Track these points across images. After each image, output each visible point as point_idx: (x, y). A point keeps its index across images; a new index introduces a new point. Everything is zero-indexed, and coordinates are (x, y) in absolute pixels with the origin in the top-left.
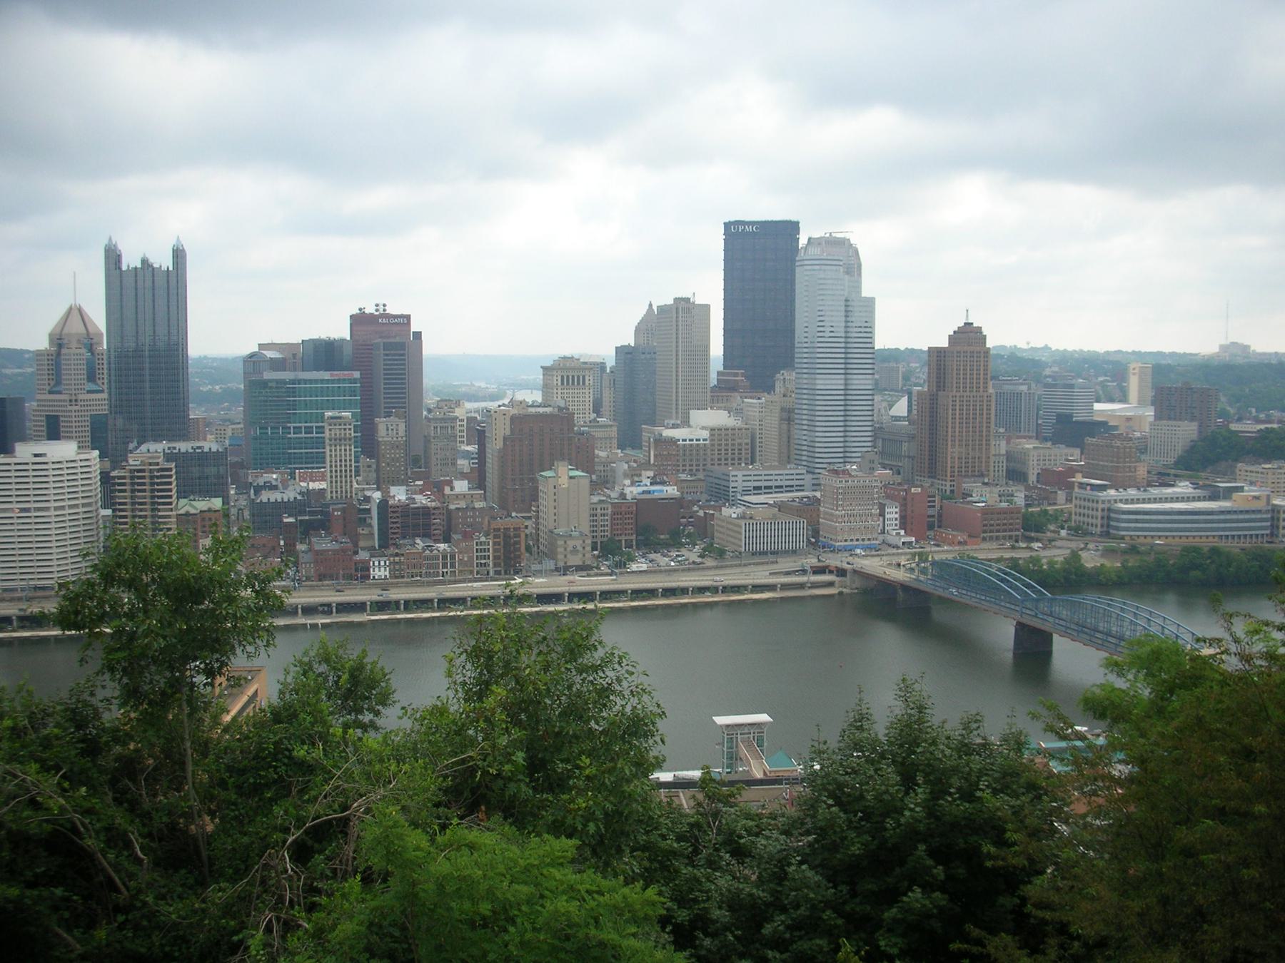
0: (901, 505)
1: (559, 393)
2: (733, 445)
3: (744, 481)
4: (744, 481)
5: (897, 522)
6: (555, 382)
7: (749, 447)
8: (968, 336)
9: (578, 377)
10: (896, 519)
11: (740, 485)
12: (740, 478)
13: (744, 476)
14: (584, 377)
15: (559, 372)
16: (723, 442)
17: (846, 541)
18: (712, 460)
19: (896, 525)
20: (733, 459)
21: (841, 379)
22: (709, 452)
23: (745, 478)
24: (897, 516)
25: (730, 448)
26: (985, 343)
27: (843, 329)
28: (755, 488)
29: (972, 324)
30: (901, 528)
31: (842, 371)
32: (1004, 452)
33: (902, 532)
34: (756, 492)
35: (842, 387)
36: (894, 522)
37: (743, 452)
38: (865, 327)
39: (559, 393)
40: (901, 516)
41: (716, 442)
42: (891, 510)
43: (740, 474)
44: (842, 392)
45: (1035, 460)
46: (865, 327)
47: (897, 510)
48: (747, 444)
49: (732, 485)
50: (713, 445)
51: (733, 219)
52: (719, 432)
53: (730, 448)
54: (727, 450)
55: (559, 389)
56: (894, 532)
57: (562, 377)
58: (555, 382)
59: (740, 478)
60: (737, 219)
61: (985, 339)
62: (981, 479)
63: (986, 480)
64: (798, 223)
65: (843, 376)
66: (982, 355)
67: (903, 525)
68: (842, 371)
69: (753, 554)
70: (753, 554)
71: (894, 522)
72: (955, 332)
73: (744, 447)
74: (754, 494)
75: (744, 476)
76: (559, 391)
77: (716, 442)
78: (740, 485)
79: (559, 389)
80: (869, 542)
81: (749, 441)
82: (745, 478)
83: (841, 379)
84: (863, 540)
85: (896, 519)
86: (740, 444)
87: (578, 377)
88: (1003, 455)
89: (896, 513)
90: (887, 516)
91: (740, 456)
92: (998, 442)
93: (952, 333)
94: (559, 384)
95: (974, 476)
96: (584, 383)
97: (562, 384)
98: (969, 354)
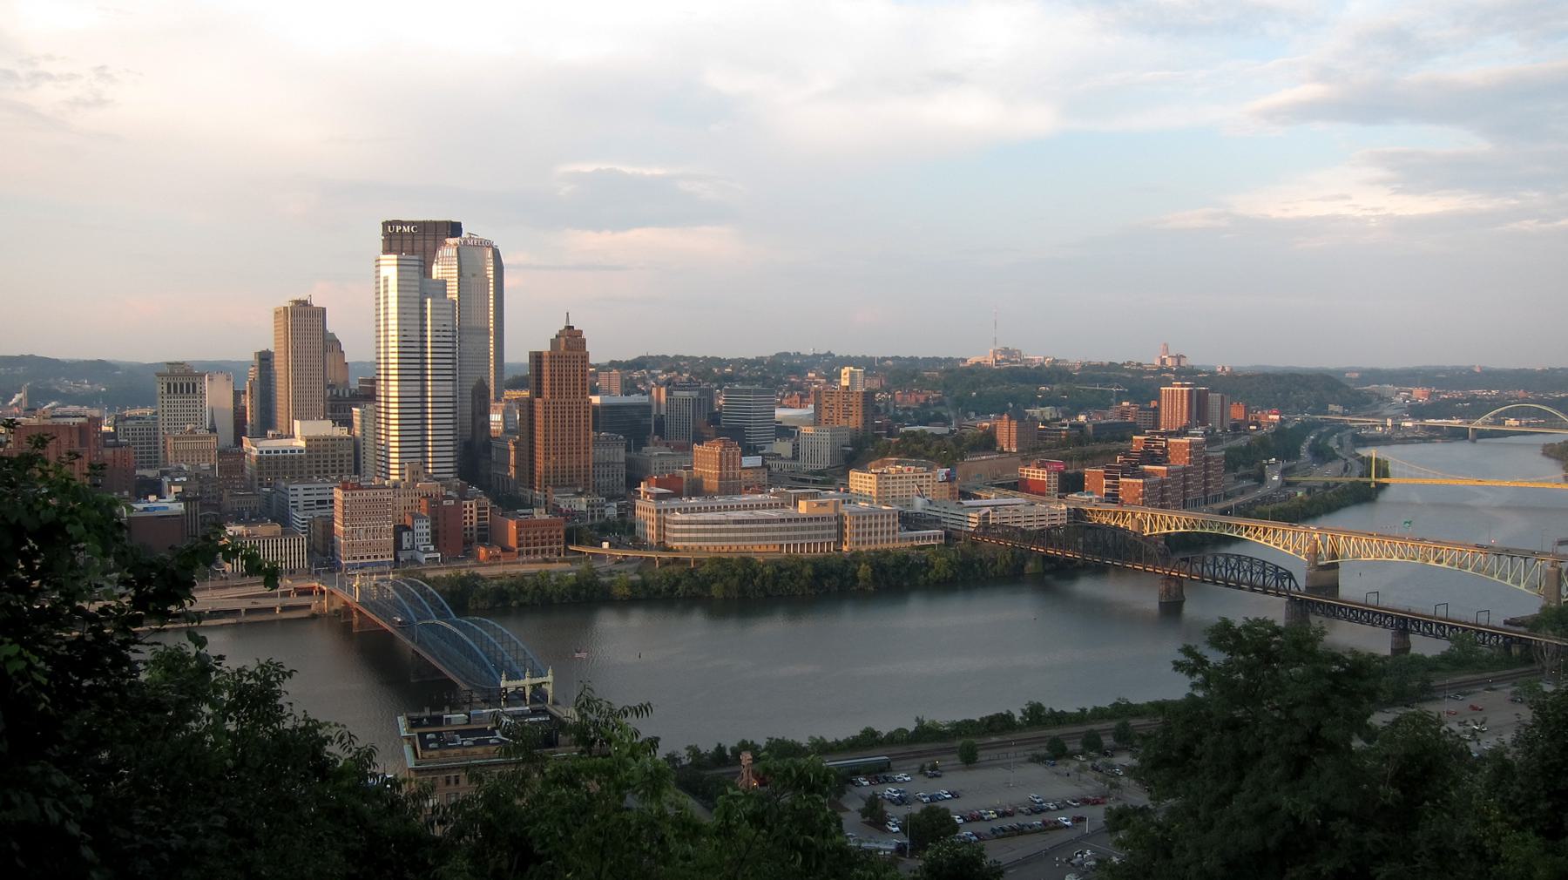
0: (432, 519)
1: (199, 406)
2: (334, 456)
3: (305, 495)
4: (305, 495)
5: (429, 537)
6: (160, 390)
7: (352, 458)
8: (571, 340)
9: (188, 385)
10: (427, 534)
11: (301, 499)
12: (301, 491)
13: (304, 489)
14: (194, 385)
15: (165, 379)
16: (321, 453)
17: (355, 558)
18: (310, 472)
19: (427, 540)
20: (326, 472)
21: (449, 386)
22: (305, 463)
23: (306, 492)
24: (428, 530)
25: (330, 459)
26: (585, 347)
27: (418, 333)
28: (319, 502)
29: (573, 327)
30: (432, 544)
31: (418, 378)
32: (623, 460)
33: (432, 548)
34: (320, 506)
35: (418, 394)
36: (425, 537)
37: (345, 463)
38: (444, 331)
39: (199, 406)
40: (432, 531)
41: (313, 454)
42: (421, 524)
43: (300, 487)
44: (418, 400)
45: (658, 469)
46: (444, 331)
47: (429, 524)
48: (349, 455)
49: (291, 499)
50: (310, 457)
51: (390, 219)
52: (317, 443)
53: (330, 459)
54: (327, 462)
55: (165, 397)
56: (422, 549)
57: (169, 385)
58: (160, 390)
59: (301, 491)
60: (400, 219)
61: (584, 343)
62: (574, 489)
63: (580, 490)
64: (460, 224)
65: (418, 383)
66: (579, 359)
67: (435, 541)
68: (418, 378)
69: (242, 575)
70: (290, 573)
71: (425, 537)
72: (557, 336)
73: (346, 458)
74: (318, 508)
75: (304, 489)
76: (165, 400)
77: (313, 454)
78: (301, 499)
79: (165, 397)
80: (381, 560)
81: (352, 451)
82: (306, 492)
83: (449, 386)
84: (376, 557)
85: (427, 534)
86: (342, 455)
87: (188, 385)
88: (622, 463)
89: (427, 527)
90: (416, 531)
91: (326, 469)
92: (616, 450)
93: (554, 337)
94: (165, 392)
95: (565, 486)
96: (194, 391)
97: (169, 392)
98: (564, 359)
